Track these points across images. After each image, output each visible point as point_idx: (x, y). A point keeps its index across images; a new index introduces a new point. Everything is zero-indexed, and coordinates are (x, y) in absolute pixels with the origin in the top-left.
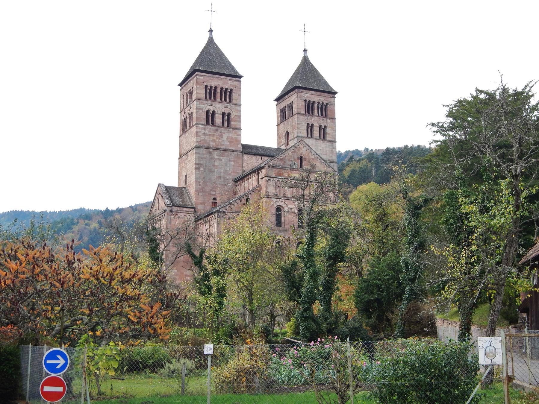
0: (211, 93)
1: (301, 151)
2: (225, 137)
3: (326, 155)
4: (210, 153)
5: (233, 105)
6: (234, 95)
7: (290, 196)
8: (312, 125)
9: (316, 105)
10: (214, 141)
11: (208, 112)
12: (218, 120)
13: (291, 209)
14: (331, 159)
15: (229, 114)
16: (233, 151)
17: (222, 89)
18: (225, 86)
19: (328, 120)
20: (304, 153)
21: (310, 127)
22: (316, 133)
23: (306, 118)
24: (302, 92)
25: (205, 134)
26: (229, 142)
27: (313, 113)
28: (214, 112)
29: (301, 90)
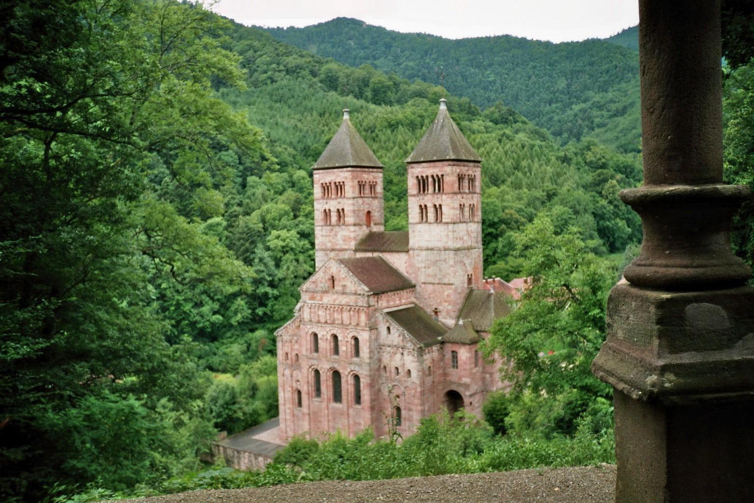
1: (332, 270)
2: (339, 237)
4: (327, 255)
5: (345, 200)
7: (323, 321)
8: (426, 206)
9: (430, 180)
10: (330, 241)
12: (334, 218)
14: (447, 246)
15: (343, 210)
16: (346, 250)
18: (337, 180)
19: (444, 197)
21: (423, 209)
25: (322, 236)
26: (344, 240)
29: (412, 165)
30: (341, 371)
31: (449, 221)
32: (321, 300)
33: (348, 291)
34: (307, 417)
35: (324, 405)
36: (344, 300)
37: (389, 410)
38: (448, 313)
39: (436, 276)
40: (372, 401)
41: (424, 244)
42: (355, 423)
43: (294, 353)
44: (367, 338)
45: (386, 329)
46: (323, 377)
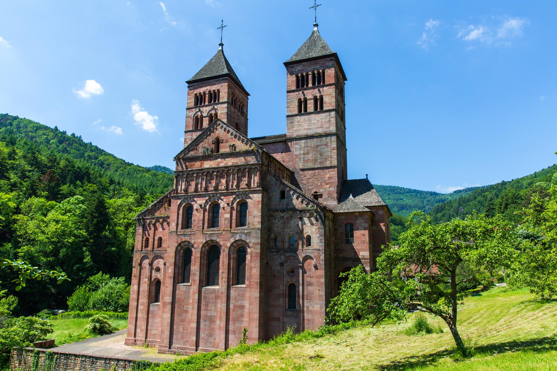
0: (199, 101)
3: (322, 127)
6: (221, 94)
11: (197, 118)
13: (201, 205)
14: (328, 131)
15: (216, 115)
17: (210, 92)
20: (221, 134)
22: (311, 106)
23: (297, 93)
24: (292, 67)
27: (307, 85)
28: (202, 117)
30: (221, 243)
31: (331, 108)
32: (201, 166)
33: (237, 150)
34: (169, 307)
35: (194, 288)
36: (230, 162)
37: (282, 288)
38: (330, 194)
39: (316, 160)
40: (262, 275)
41: (303, 133)
42: (235, 306)
43: (157, 238)
44: (260, 199)
45: (279, 192)
46: (196, 254)
